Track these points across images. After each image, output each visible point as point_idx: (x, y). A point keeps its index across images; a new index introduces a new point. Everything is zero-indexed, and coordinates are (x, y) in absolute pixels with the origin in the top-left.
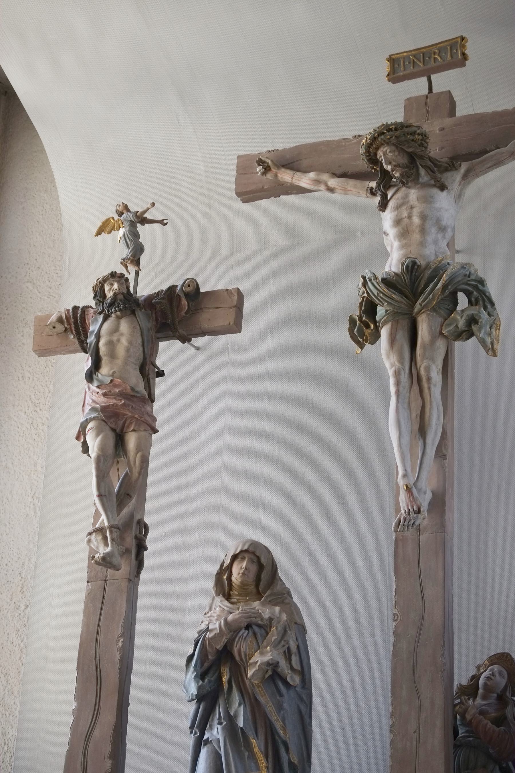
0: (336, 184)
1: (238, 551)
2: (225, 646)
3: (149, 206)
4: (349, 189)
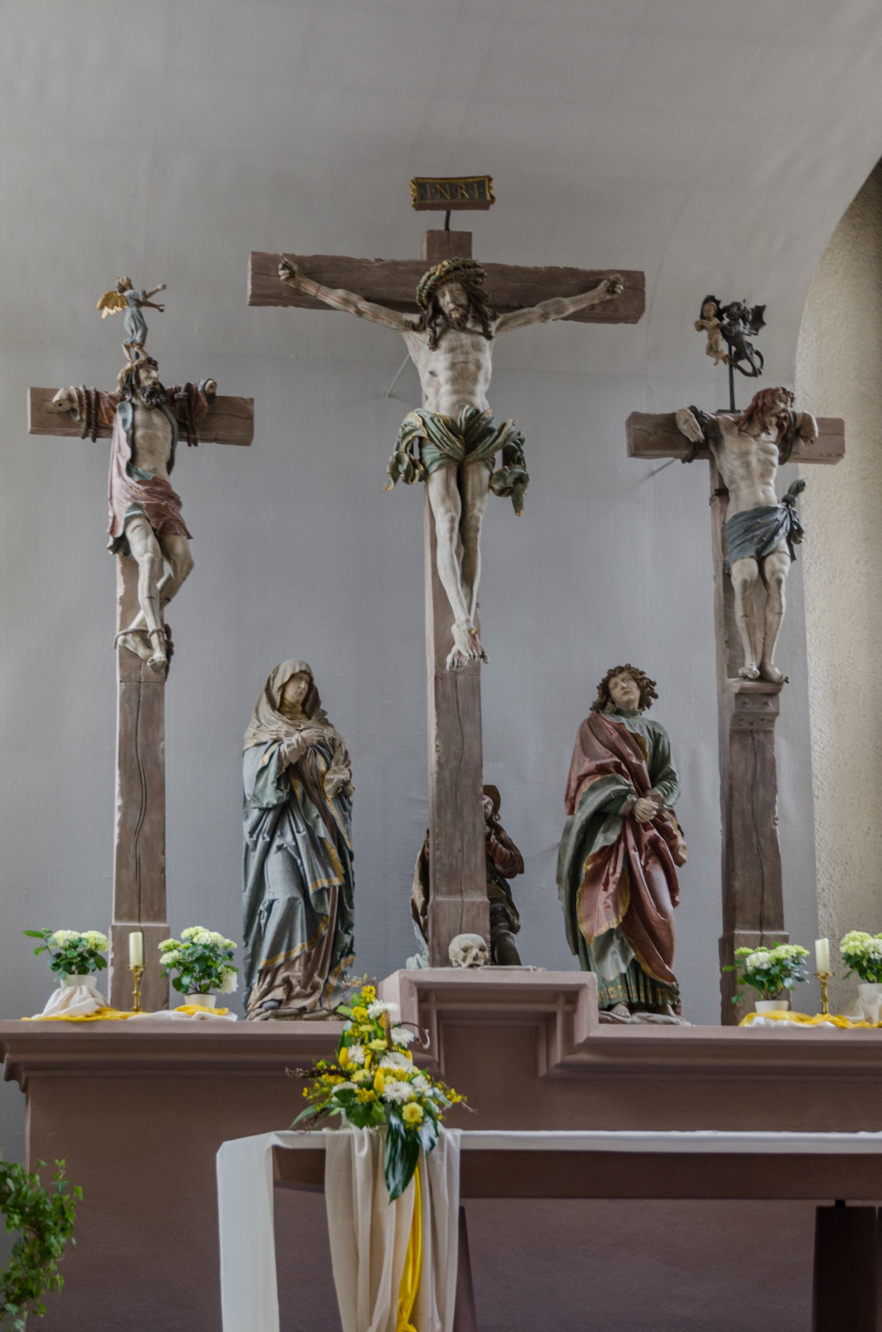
0: (368, 308)
1: (297, 670)
2: (297, 763)
3: (159, 286)
4: (382, 316)
